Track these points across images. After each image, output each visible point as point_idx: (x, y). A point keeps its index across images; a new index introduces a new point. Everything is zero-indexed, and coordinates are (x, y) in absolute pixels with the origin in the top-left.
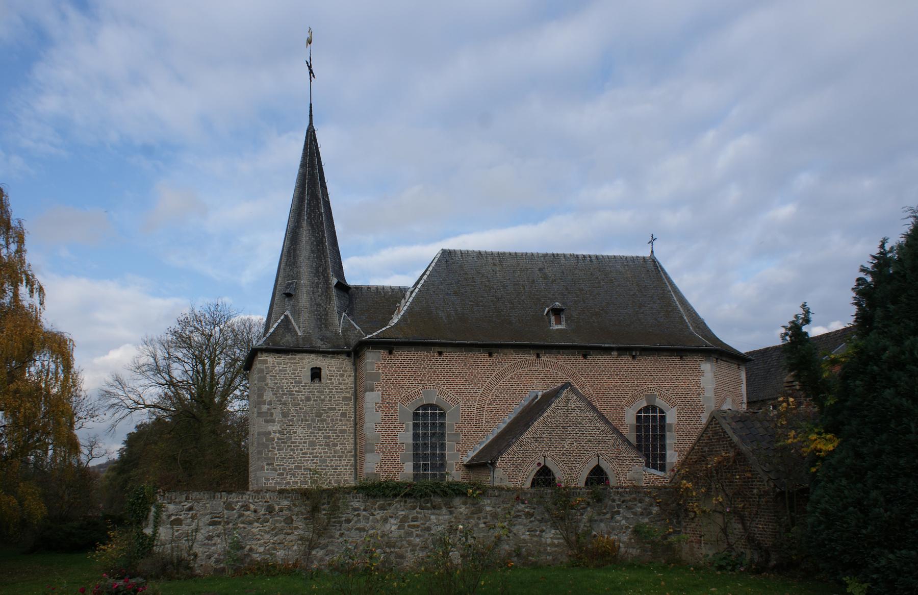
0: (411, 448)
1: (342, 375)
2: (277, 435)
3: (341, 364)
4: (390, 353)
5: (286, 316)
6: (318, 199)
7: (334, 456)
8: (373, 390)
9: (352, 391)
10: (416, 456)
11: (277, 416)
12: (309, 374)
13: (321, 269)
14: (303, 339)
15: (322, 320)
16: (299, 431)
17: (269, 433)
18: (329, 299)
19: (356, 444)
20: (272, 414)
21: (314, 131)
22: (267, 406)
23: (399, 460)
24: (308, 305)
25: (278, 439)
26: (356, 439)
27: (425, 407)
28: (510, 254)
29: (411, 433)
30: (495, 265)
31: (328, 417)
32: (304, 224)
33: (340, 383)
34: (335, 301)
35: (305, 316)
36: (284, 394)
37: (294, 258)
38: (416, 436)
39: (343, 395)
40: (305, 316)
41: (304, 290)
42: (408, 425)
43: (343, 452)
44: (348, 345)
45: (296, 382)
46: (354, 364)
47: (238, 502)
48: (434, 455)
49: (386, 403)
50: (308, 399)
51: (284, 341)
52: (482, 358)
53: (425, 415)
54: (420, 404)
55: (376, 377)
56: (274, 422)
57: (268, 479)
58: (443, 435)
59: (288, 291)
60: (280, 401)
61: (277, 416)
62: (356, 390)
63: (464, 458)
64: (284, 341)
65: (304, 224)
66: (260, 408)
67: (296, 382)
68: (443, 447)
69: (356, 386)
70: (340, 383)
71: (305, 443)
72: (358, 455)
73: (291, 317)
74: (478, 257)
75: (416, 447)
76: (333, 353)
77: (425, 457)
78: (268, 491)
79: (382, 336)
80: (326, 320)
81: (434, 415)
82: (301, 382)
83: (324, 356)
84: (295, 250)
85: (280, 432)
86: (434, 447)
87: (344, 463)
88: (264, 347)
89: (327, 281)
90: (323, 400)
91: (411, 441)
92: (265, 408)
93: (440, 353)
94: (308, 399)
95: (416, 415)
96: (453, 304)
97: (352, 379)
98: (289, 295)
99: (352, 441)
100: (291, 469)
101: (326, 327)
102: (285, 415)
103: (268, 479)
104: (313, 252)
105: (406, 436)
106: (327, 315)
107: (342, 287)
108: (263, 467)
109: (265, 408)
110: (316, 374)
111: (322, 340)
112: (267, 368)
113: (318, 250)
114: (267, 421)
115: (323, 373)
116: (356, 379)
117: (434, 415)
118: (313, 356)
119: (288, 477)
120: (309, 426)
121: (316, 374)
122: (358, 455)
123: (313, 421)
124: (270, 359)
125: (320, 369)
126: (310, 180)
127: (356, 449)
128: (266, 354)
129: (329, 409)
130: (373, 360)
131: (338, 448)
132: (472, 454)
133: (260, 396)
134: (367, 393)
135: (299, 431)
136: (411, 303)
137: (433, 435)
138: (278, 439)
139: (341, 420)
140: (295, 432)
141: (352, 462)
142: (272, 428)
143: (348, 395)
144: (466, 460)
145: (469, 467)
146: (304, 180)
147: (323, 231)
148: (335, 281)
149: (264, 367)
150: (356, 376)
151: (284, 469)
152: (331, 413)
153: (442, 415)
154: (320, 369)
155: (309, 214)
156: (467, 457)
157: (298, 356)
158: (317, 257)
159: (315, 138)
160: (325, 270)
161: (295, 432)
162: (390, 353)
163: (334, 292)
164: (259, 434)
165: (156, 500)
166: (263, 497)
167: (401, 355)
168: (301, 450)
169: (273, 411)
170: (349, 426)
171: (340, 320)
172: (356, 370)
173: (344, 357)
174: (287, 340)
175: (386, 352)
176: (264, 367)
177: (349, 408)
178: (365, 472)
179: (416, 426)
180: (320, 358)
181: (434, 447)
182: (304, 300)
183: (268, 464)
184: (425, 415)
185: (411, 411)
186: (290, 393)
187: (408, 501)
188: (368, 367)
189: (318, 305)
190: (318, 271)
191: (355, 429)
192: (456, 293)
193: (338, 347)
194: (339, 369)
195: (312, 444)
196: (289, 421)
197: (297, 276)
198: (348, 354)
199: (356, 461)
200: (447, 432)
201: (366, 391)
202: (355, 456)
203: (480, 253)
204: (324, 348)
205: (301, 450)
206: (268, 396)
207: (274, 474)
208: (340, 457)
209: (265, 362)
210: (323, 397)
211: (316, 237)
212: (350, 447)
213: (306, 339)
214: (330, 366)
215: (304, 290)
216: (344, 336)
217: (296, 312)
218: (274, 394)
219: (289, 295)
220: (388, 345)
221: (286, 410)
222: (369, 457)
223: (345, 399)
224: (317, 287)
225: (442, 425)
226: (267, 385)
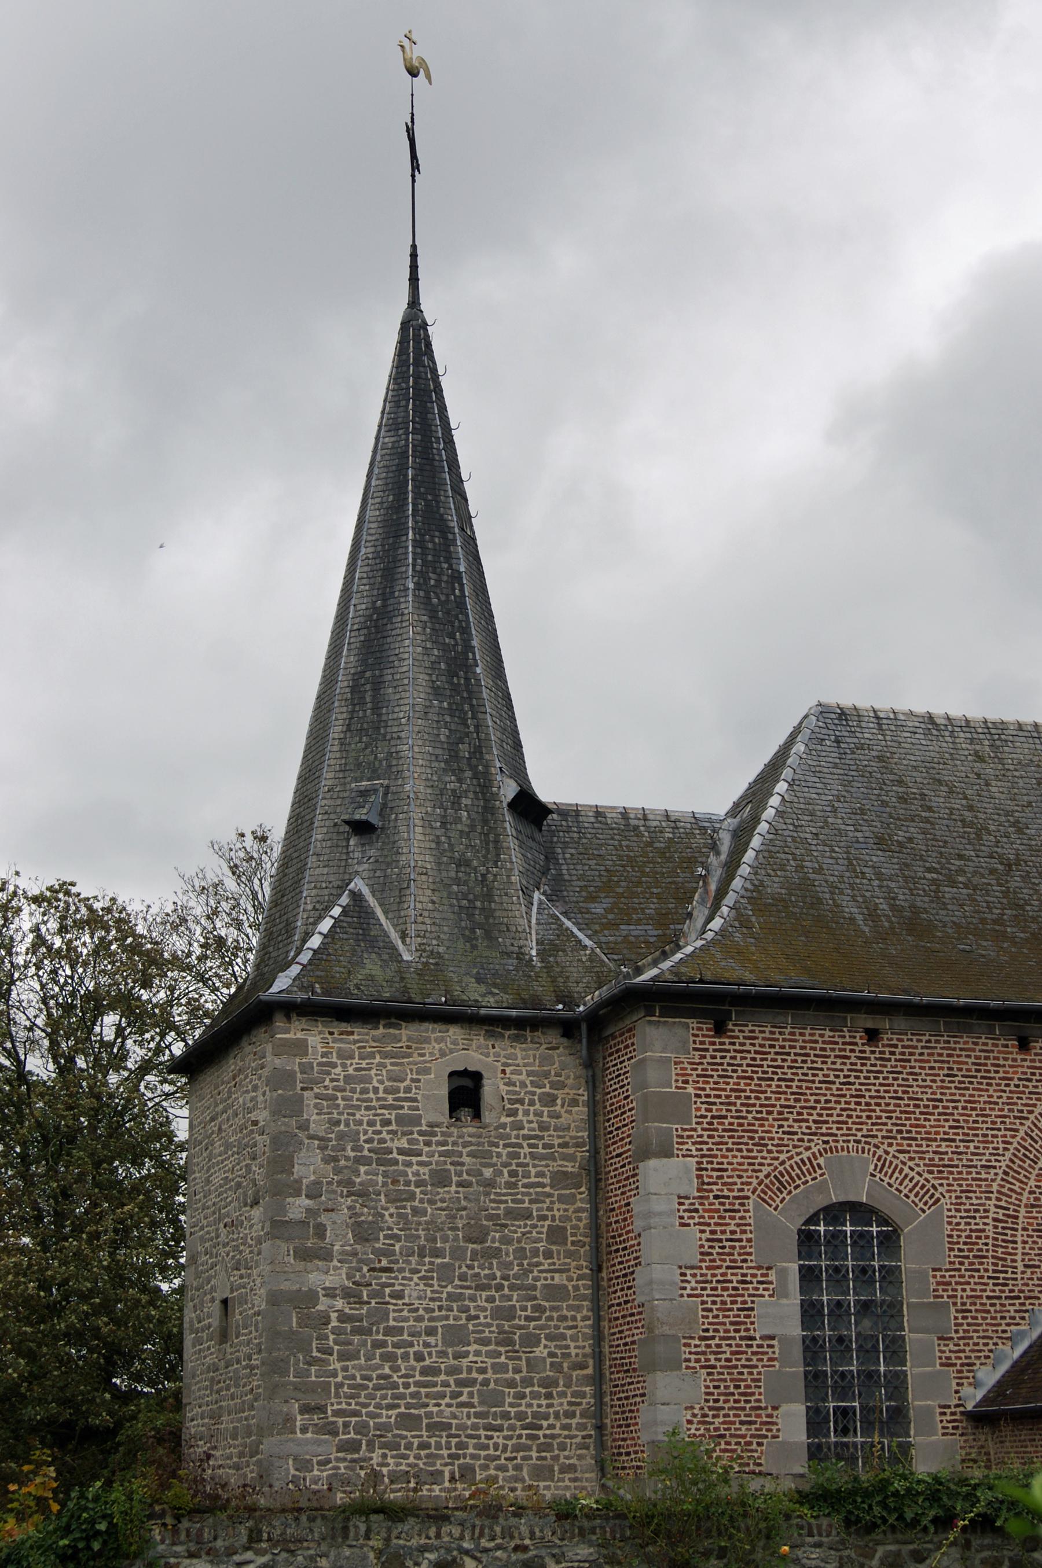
0: (797, 1352)
1: (549, 1100)
2: (339, 1304)
3: (545, 1060)
4: (720, 1029)
5: (357, 897)
6: (445, 530)
7: (527, 1382)
8: (668, 1154)
9: (582, 1154)
10: (814, 1380)
11: (339, 1237)
12: (444, 1091)
13: (464, 750)
14: (420, 974)
15: (477, 915)
16: (414, 1288)
17: (312, 1297)
18: (493, 846)
19: (598, 1337)
20: (320, 1231)
21: (425, 325)
22: (304, 1202)
23: (761, 1395)
24: (428, 861)
25: (343, 1318)
26: (598, 1319)
27: (834, 1212)
28: (1020, 726)
29: (794, 1300)
30: (979, 758)
31: (506, 1241)
32: (409, 605)
33: (543, 1127)
34: (514, 855)
35: (420, 898)
36: (359, 1161)
37: (376, 709)
38: (810, 1313)
39: (554, 1166)
40: (420, 898)
41: (417, 814)
42: (783, 1273)
43: (557, 1367)
44: (570, 1002)
45: (400, 1120)
46: (589, 1064)
47: (423, 1549)
48: (870, 1376)
49: (712, 1200)
50: (441, 1179)
51: (360, 976)
52: (996, 1050)
53: (835, 1239)
54: (820, 1202)
55: (675, 1107)
56: (328, 1257)
57: (304, 1465)
58: (893, 1310)
59: (361, 815)
60: (350, 1183)
61: (339, 1237)
62: (595, 1152)
63: (967, 1390)
64: (360, 976)
65: (409, 605)
66: (282, 1209)
67: (400, 1120)
68: (896, 1351)
69: (594, 1137)
70: (543, 1127)
71: (431, 1332)
72: (611, 1377)
73: (372, 901)
74: (927, 732)
75: (812, 1348)
76: (520, 1024)
77: (843, 1386)
78: (520, 1510)
79: (668, 976)
80: (488, 913)
81: (862, 1239)
82: (416, 1121)
83: (490, 1034)
84: (378, 685)
85: (348, 1294)
86: (868, 1352)
87: (561, 1404)
88: (300, 996)
89: (485, 788)
90: (490, 1184)
91: (795, 1330)
92: (298, 1206)
93: (872, 1036)
94: (441, 1179)
95: (807, 1239)
96: (880, 876)
97: (581, 1111)
98: (362, 828)
99: (585, 1327)
100: (385, 1427)
101: (488, 935)
102: (364, 1233)
103: (304, 1465)
104: (437, 692)
105: (780, 1314)
106: (489, 897)
107: (529, 807)
108: (289, 1419)
109: (298, 1206)
110: (466, 1093)
111: (479, 980)
112: (306, 1068)
113: (455, 689)
114: (304, 1255)
115: (491, 1090)
116: (593, 1115)
117: (862, 1239)
118: (455, 1032)
119: (376, 1457)
120: (445, 1274)
121: (466, 1093)
122: (611, 1377)
123: (457, 1254)
124: (316, 1039)
125: (477, 1077)
126: (419, 470)
127: (598, 1357)
128: (303, 1023)
129: (509, 1212)
130: (662, 1055)
131: (541, 1351)
132: (989, 1376)
133: (282, 1162)
134: (653, 1163)
135: (414, 1288)
136: (755, 869)
137: (865, 1307)
138: (343, 1318)
139: (548, 1254)
140: (398, 1295)
141: (589, 1400)
142: (323, 1278)
143: (570, 1167)
144: (973, 1397)
145: (981, 1419)
146: (402, 468)
147: (466, 631)
148: (509, 790)
149: (294, 1064)
150: (594, 1106)
151: (362, 1429)
152: (517, 1229)
153: (890, 1241)
154: (477, 1077)
155: (422, 578)
156: (976, 1384)
157: (407, 1032)
158: (451, 712)
159: (429, 345)
160: (479, 751)
161: (398, 1295)
162: (720, 1029)
163: (509, 822)
164: (275, 1299)
165: (148, 1542)
166: (508, 1533)
167: (751, 1036)
168: (419, 1357)
169: (323, 1218)
170: (574, 1276)
171: (528, 914)
172: (593, 1083)
173: (553, 1037)
174: (368, 978)
175: (707, 1026)
176: (294, 1064)
177: (574, 1211)
178: (644, 1438)
179: (809, 1277)
180: (480, 1039)
181: (868, 1352)
182: (415, 843)
183: (305, 1409)
184: (835, 1239)
185: (793, 1225)
186: (382, 1157)
187: (976, 1542)
188: (652, 1074)
189: (462, 863)
190: (454, 755)
191: (597, 1287)
192: (881, 842)
193: (535, 1003)
194: (539, 1077)
195: (456, 1336)
196: (380, 1253)
197: (391, 768)
198: (568, 1028)
199: (599, 1395)
200: (909, 1298)
201: (645, 1154)
202: (598, 1379)
203: (930, 718)
204: (491, 1003)
205: (419, 1357)
206: (309, 1165)
207: (329, 1448)
208: (548, 1383)
209: (301, 1048)
210: (488, 1173)
211: (445, 648)
212: (579, 1347)
213: (432, 968)
214: (509, 1068)
215: (417, 814)
216: (548, 968)
217: (393, 889)
218: (327, 1160)
219: (362, 828)
220: (711, 1005)
221: (366, 1216)
222: (664, 1385)
223: (560, 1179)
224: (456, 804)
225: (891, 1276)
226: (304, 1126)
